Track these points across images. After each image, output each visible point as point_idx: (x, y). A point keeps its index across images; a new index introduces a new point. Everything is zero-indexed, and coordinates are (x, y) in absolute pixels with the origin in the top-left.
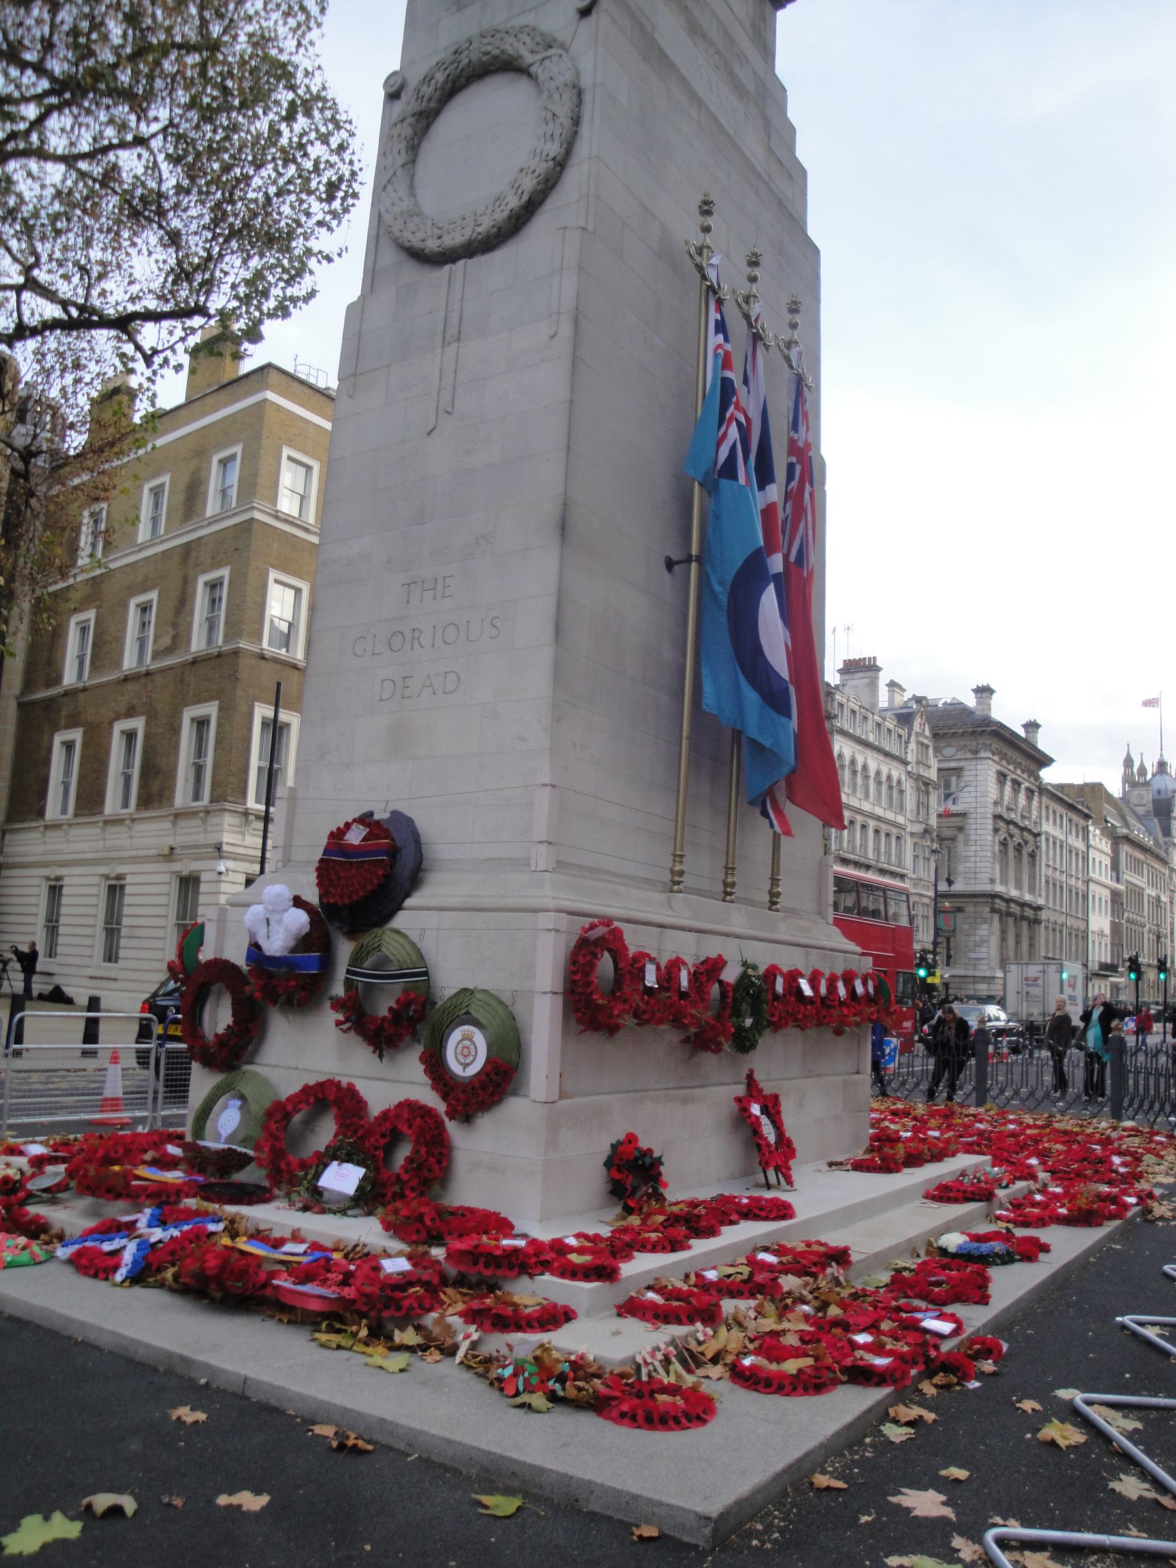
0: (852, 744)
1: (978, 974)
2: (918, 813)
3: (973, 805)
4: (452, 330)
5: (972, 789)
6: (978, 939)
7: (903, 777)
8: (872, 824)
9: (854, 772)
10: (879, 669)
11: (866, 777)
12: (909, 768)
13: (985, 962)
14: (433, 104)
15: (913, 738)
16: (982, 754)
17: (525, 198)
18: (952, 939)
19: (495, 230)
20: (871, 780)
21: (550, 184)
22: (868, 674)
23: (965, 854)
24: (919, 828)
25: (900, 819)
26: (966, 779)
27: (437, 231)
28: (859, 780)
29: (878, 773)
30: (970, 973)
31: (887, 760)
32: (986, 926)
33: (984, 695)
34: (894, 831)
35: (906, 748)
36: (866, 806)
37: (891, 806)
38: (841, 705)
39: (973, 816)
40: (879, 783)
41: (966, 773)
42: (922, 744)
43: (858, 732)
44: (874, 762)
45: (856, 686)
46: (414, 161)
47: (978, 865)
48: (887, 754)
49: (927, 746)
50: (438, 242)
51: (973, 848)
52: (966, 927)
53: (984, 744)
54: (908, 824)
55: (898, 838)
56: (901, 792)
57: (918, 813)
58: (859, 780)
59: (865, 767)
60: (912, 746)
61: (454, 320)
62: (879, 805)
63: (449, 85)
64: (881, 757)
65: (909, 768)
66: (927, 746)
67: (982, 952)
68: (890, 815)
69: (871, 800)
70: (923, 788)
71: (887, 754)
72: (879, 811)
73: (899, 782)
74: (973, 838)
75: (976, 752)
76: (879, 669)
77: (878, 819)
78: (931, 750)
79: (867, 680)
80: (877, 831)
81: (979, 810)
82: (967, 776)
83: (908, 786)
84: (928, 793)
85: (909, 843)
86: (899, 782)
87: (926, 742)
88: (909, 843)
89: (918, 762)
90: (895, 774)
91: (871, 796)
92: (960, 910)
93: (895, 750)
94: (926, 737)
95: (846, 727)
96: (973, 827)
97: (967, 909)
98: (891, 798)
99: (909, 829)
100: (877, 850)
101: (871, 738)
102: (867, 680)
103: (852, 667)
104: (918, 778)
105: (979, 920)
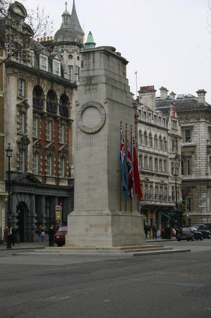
1: (203, 214)
2: (173, 150)
3: (198, 142)
5: (197, 135)
6: (202, 199)
7: (166, 136)
8: (154, 156)
9: (146, 137)
11: (151, 138)
12: (169, 132)
13: (205, 209)
15: (170, 119)
16: (201, 120)
18: (191, 200)
20: (153, 139)
22: (151, 93)
23: (195, 163)
24: (173, 156)
25: (166, 154)
26: (195, 131)
28: (148, 140)
29: (156, 136)
30: (199, 214)
31: (159, 130)
32: (205, 194)
33: (202, 94)
34: (163, 158)
35: (167, 123)
36: (151, 150)
38: (140, 111)
39: (198, 147)
40: (156, 140)
41: (195, 128)
42: (174, 121)
43: (147, 121)
44: (154, 132)
45: (146, 98)
47: (201, 168)
48: (159, 128)
49: (176, 122)
51: (198, 161)
52: (197, 194)
53: (202, 116)
54: (169, 155)
55: (165, 161)
57: (173, 150)
58: (148, 140)
59: (150, 134)
60: (170, 122)
64: (157, 129)
65: (169, 132)
66: (176, 122)
67: (204, 205)
69: (153, 147)
70: (175, 139)
71: (159, 128)
72: (156, 151)
73: (164, 138)
74: (198, 156)
75: (198, 119)
77: (157, 154)
78: (178, 123)
79: (150, 96)
81: (201, 144)
82: (195, 130)
84: (177, 141)
86: (164, 138)
87: (175, 120)
88: (170, 162)
89: (172, 129)
90: (163, 136)
91: (153, 145)
92: (194, 187)
93: (162, 125)
94: (175, 118)
95: (142, 119)
96: (198, 151)
97: (197, 187)
98: (161, 145)
99: (169, 157)
100: (156, 166)
101: (152, 122)
102: (150, 96)
103: (144, 90)
104: (173, 135)
105: (202, 191)
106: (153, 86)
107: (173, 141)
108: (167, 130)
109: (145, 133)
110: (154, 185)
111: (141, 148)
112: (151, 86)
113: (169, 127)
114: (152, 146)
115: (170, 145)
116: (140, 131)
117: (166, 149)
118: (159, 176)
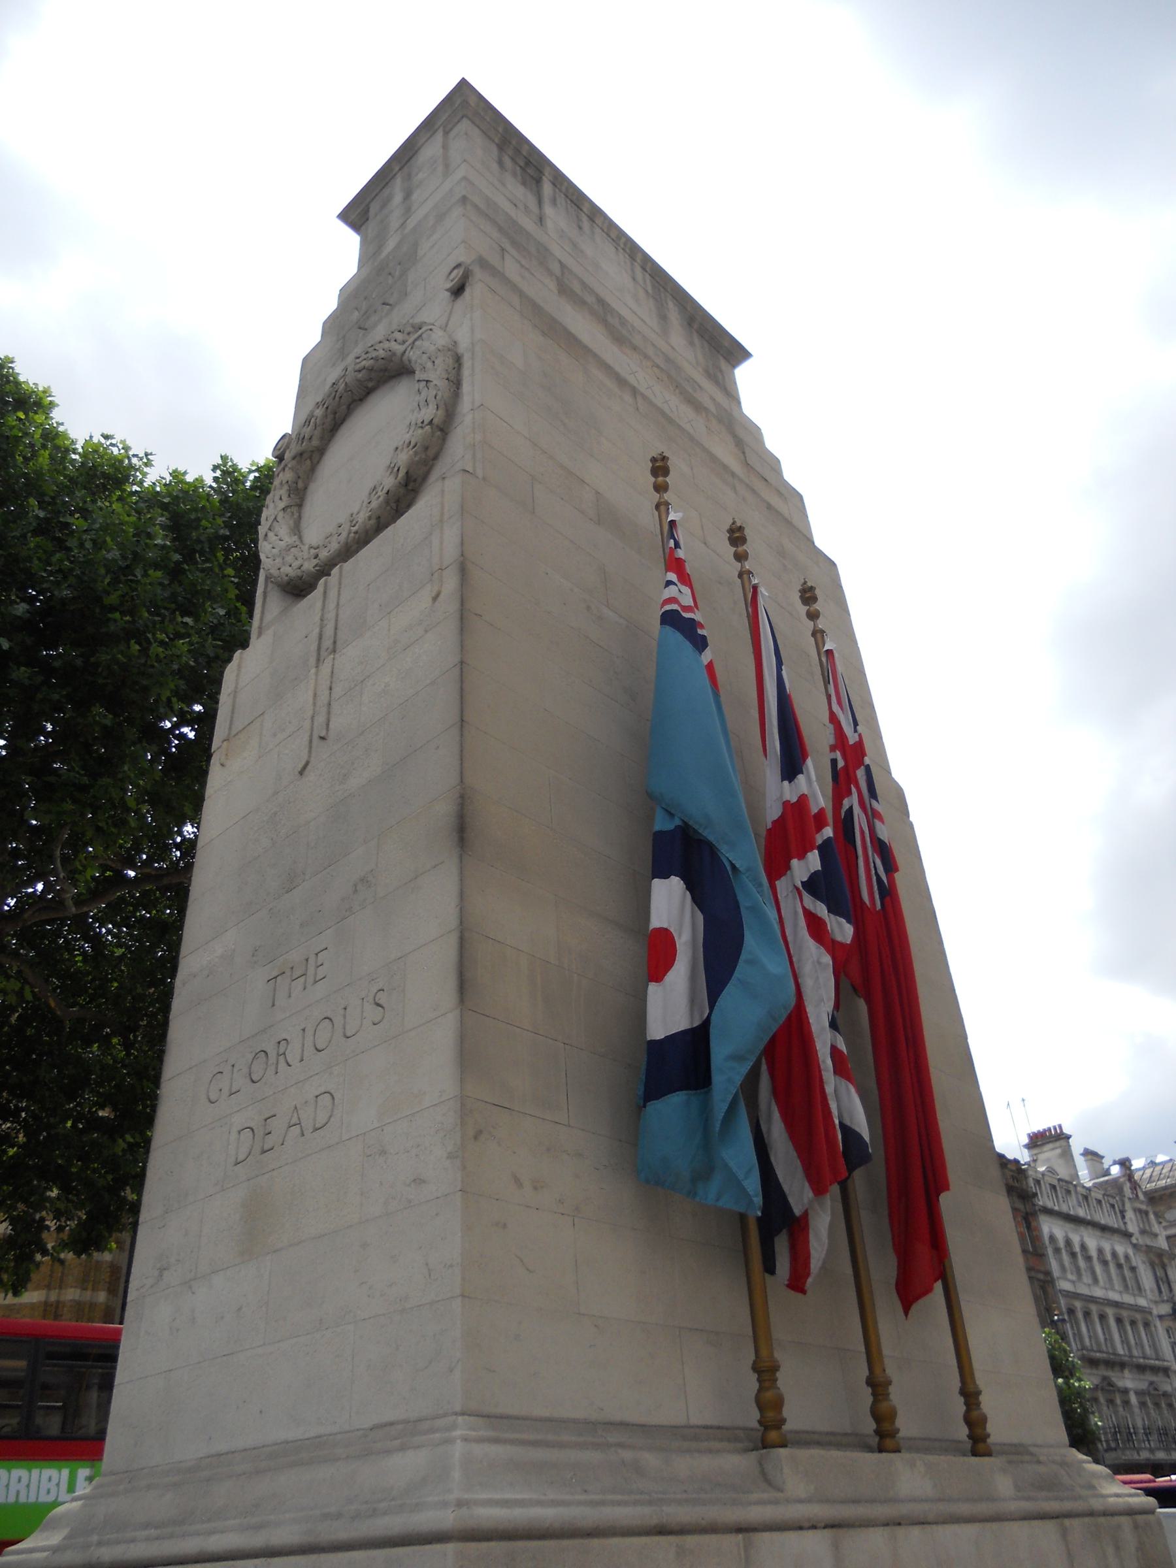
0: (1061, 1222)
4: (327, 643)
7: (1130, 1252)
8: (1110, 1312)
9: (1073, 1255)
10: (1068, 1137)
11: (1088, 1259)
12: (1134, 1240)
14: (315, 442)
15: (1128, 1206)
17: (402, 474)
19: (373, 522)
21: (431, 453)
25: (1142, 1302)
27: (313, 551)
28: (1082, 1263)
29: (1100, 1251)
31: (1107, 1235)
34: (1138, 1316)
35: (1123, 1217)
36: (1098, 1292)
37: (1126, 1287)
38: (1038, 1182)
40: (1105, 1263)
42: (1140, 1211)
43: (1064, 1208)
44: (1093, 1241)
46: (300, 506)
48: (1104, 1229)
49: (1147, 1213)
50: (315, 562)
54: (1152, 1306)
56: (1133, 1269)
58: (1082, 1263)
59: (1083, 1247)
60: (1130, 1214)
61: (329, 631)
62: (1113, 1289)
63: (330, 417)
64: (1098, 1233)
65: (1134, 1240)
68: (1128, 1299)
69: (1101, 1283)
71: (1104, 1229)
72: (1114, 1296)
73: (1127, 1257)
76: (1068, 1137)
77: (1116, 1305)
78: (1152, 1216)
79: (1059, 1151)
80: (1119, 1321)
83: (1138, 1261)
84: (1164, 1267)
85: (1160, 1328)
87: (1144, 1207)
88: (1160, 1328)
89: (1143, 1232)
90: (1120, 1249)
91: (1100, 1277)
94: (1142, 1202)
95: (1049, 1204)
98: (1124, 1279)
99: (1155, 1312)
100: (1125, 1341)
101: (1081, 1213)
103: (1038, 1140)
104: (1149, 1249)
106: (1060, 1126)
107: (1152, 1265)
108: (1127, 1235)
109: (1068, 1243)
110: (1133, 1399)
111: (1065, 1285)
112: (1055, 1128)
113: (1132, 1227)
114: (1095, 1280)
115: (1147, 1279)
116: (1052, 1238)
117: (1139, 1289)
118: (1141, 1369)
